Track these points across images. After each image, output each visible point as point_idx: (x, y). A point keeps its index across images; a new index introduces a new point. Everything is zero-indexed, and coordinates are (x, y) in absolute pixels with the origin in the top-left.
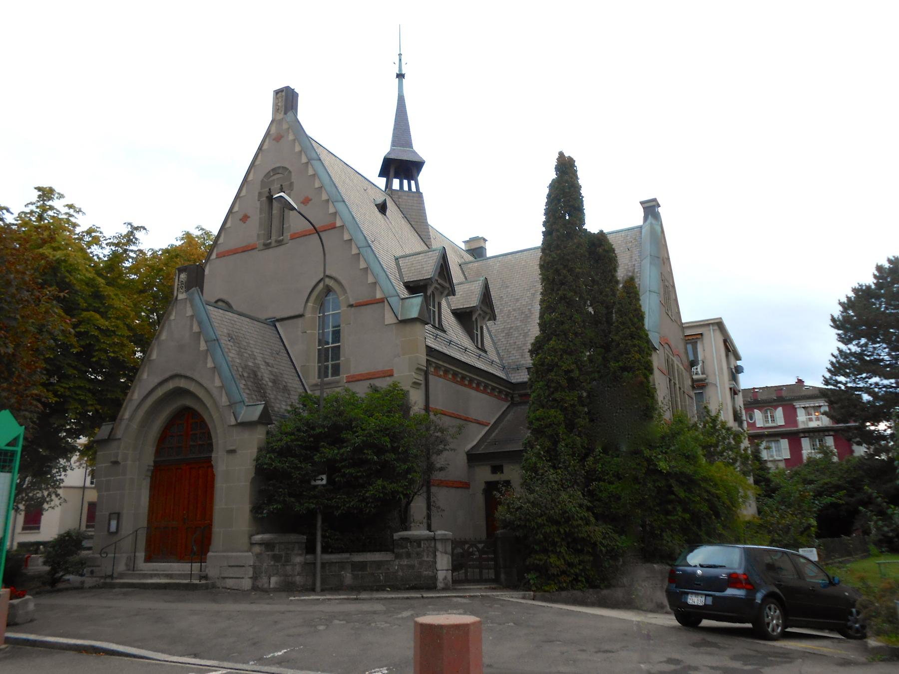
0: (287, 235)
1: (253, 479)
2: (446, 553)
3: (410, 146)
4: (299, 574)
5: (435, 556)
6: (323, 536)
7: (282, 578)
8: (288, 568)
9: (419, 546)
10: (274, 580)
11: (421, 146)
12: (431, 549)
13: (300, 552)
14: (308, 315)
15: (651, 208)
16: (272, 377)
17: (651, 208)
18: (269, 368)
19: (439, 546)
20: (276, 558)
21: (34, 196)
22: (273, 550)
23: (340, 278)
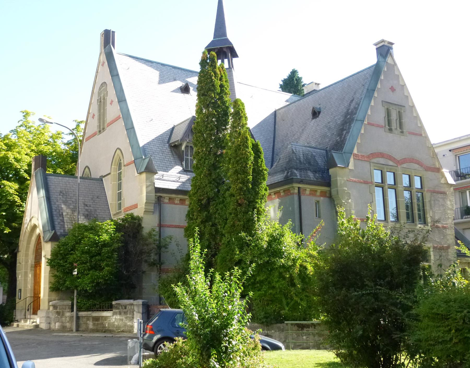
0: (106, 125)
1: (50, 271)
2: (139, 312)
3: (226, 36)
4: (68, 322)
5: (133, 314)
6: (77, 302)
7: (61, 324)
8: (64, 318)
9: (126, 308)
10: (57, 324)
11: (233, 36)
12: (131, 310)
13: (69, 310)
14: (112, 173)
15: (384, 50)
16: (86, 213)
17: (384, 50)
18: (86, 208)
19: (136, 308)
20: (58, 313)
21: (21, 116)
22: (56, 309)
23: (122, 149)
